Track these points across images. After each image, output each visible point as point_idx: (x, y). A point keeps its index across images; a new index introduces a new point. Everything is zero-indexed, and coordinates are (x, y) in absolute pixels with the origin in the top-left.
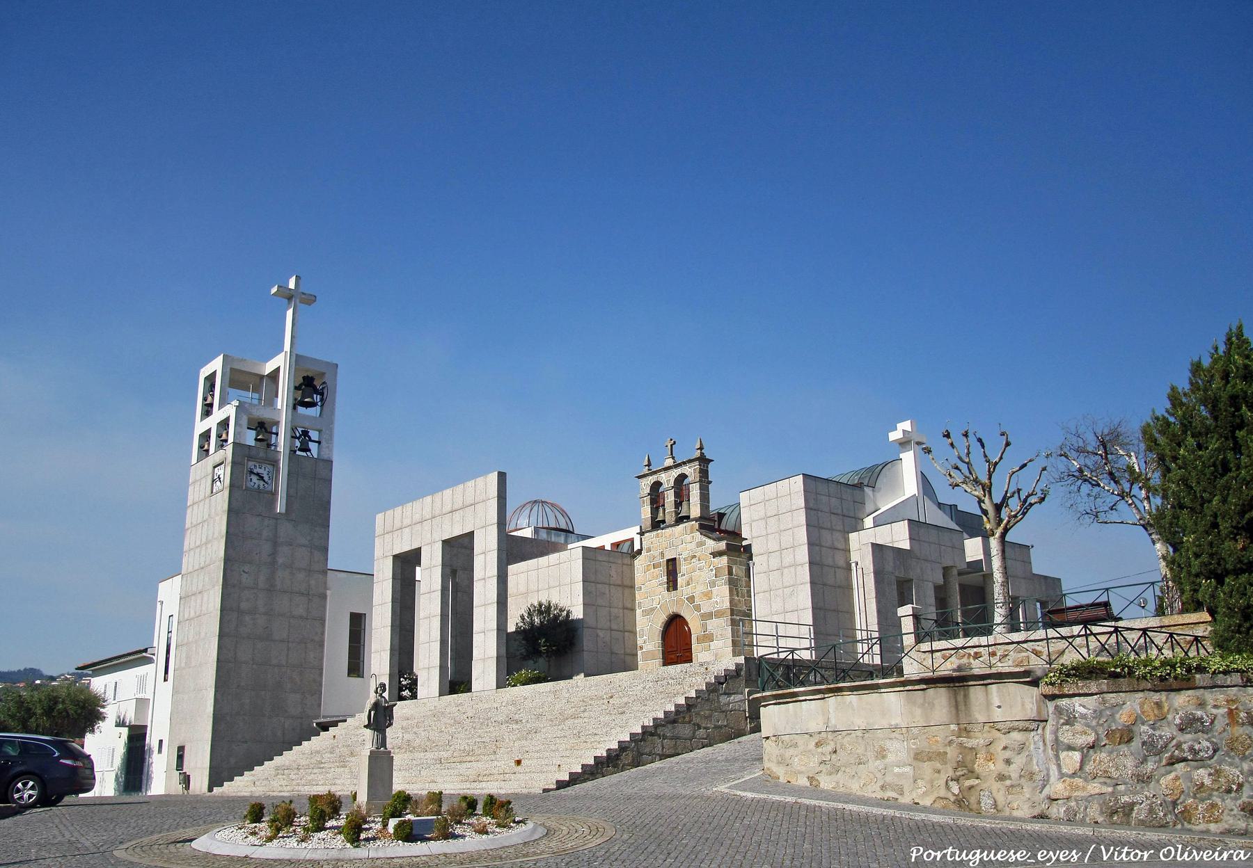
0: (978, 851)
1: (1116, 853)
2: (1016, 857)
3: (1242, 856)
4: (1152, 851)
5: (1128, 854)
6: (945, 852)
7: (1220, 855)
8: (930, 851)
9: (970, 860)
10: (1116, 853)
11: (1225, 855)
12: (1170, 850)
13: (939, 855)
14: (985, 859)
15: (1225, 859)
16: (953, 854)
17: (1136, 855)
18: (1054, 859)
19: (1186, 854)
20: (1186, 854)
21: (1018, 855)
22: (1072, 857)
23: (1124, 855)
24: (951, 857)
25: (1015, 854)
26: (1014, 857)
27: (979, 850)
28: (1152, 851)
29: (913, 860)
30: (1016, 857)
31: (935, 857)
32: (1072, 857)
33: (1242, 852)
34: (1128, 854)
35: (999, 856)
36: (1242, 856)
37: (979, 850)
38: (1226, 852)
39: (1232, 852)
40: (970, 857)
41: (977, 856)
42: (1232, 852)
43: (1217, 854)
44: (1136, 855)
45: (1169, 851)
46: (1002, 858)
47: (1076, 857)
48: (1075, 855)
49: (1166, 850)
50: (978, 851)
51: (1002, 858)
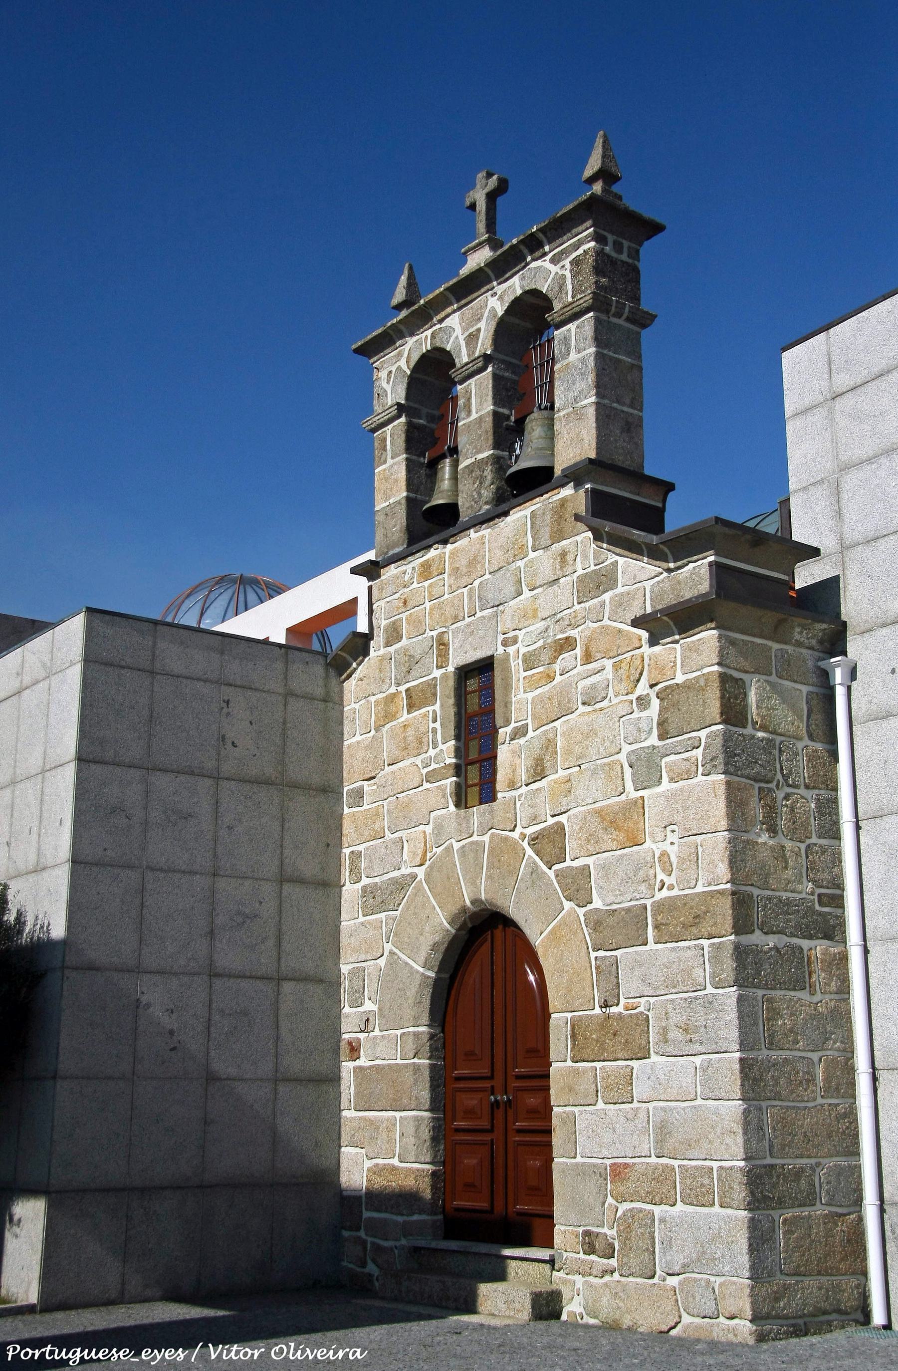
0: (79, 1350)
1: (225, 1352)
2: (119, 1356)
3: (358, 1354)
4: (263, 1350)
5: (237, 1353)
6: (43, 1350)
7: (335, 1354)
8: (28, 1349)
9: (69, 1359)
10: (225, 1352)
11: (341, 1354)
12: (281, 1348)
13: (37, 1353)
14: (86, 1358)
15: (340, 1358)
16: (52, 1353)
17: (245, 1354)
18: (159, 1357)
19: (299, 1352)
20: (299, 1352)
21: (121, 1353)
22: (179, 1355)
23: (233, 1354)
24: (50, 1356)
25: (117, 1352)
26: (116, 1356)
27: (80, 1349)
28: (263, 1350)
29: (9, 1359)
30: (119, 1356)
31: (33, 1355)
32: (179, 1355)
33: (359, 1350)
34: (237, 1353)
35: (100, 1355)
36: (358, 1354)
37: (80, 1349)
38: (341, 1350)
39: (348, 1350)
40: (70, 1355)
41: (76, 1355)
42: (348, 1350)
43: (331, 1352)
44: (245, 1354)
45: (281, 1349)
46: (103, 1356)
47: (182, 1356)
48: (181, 1354)
49: (277, 1348)
50: (79, 1350)
51: (103, 1356)
